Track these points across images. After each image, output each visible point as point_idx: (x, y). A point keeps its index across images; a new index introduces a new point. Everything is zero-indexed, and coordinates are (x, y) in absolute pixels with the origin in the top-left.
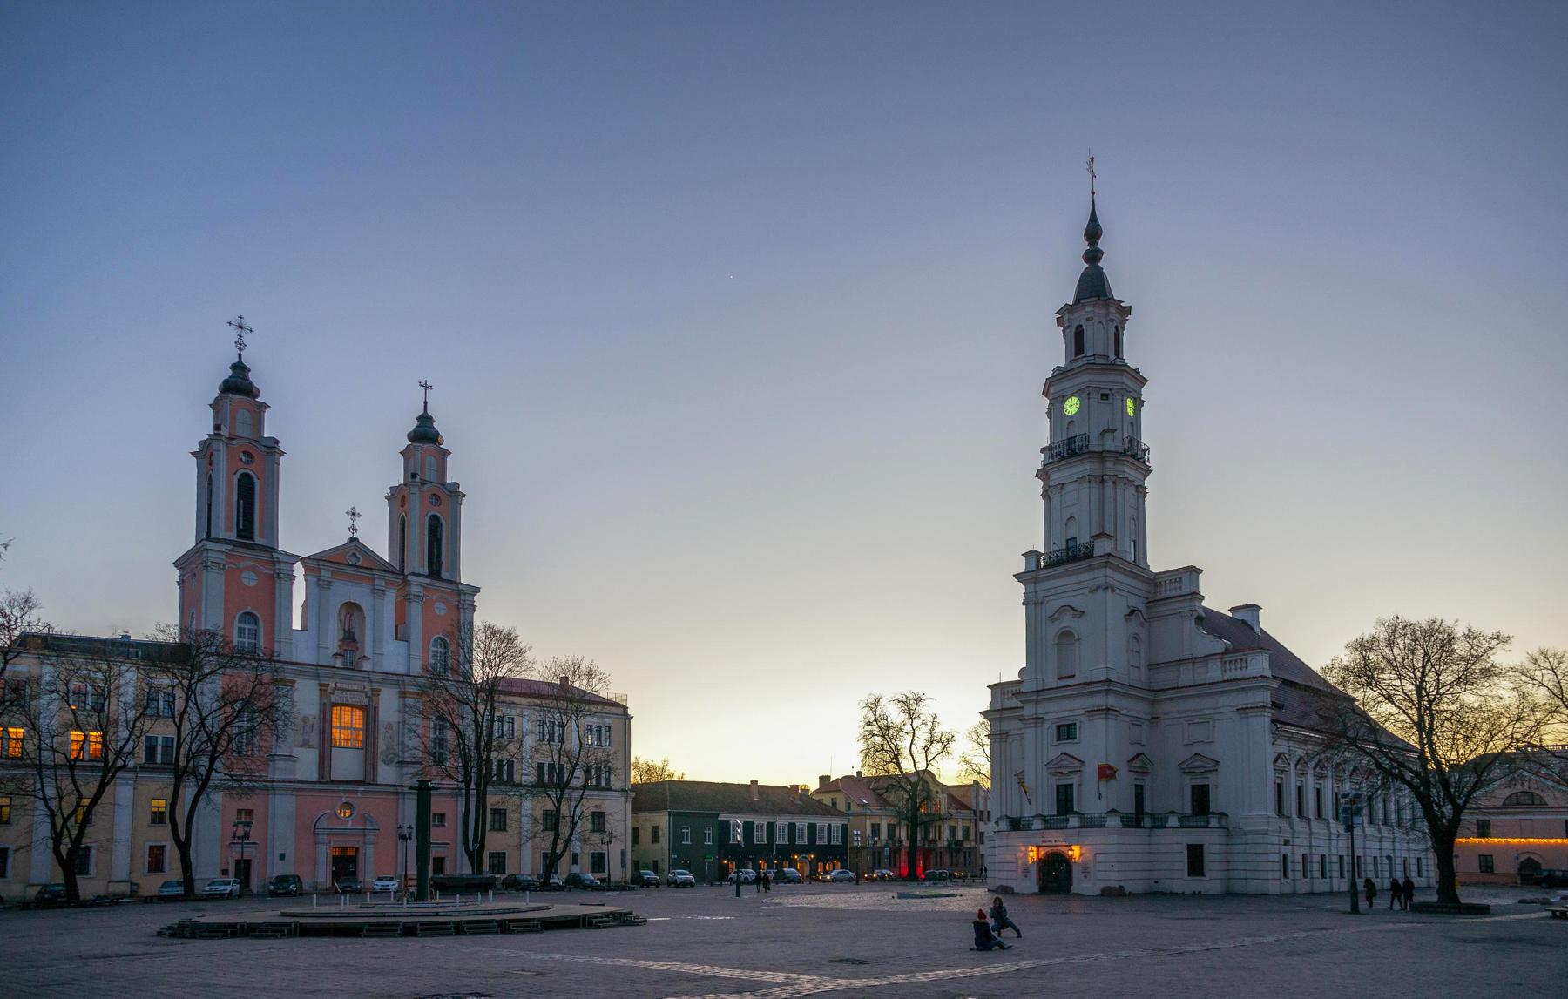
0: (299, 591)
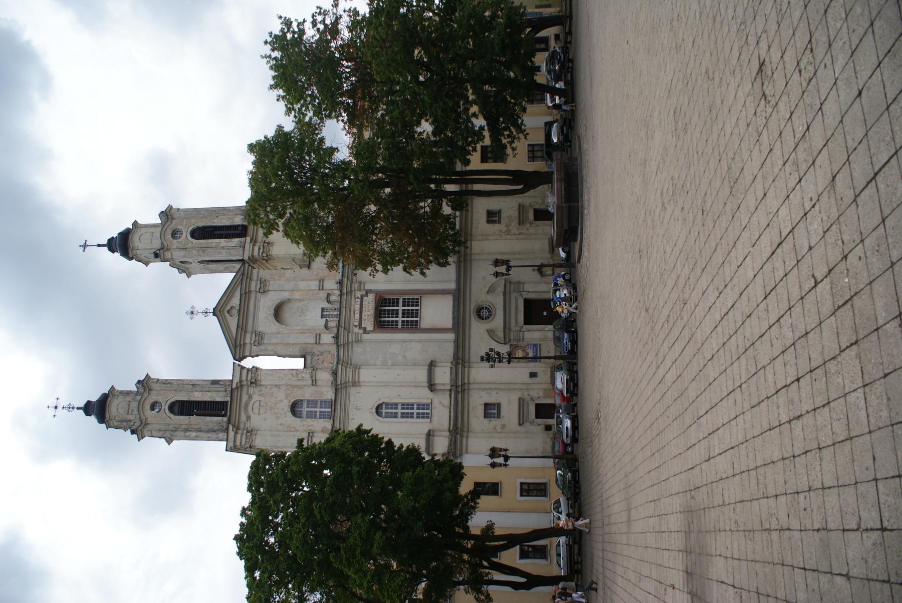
0: (266, 362)
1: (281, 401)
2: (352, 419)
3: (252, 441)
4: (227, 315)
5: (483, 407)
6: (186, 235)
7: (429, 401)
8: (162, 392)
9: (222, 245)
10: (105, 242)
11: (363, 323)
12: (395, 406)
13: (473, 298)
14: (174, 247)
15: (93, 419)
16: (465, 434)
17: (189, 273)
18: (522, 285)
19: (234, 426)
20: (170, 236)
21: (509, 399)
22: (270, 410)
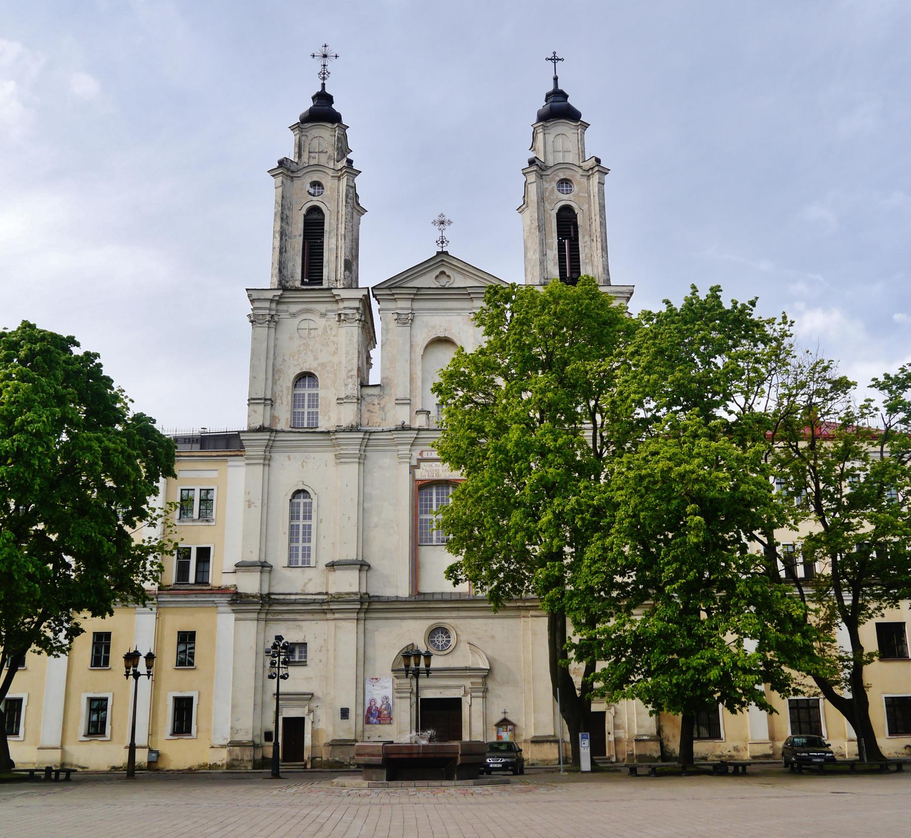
1: (316, 358)
2: (289, 458)
3: (260, 324)
4: (437, 272)
5: (301, 641)
6: (565, 199)
7: (312, 564)
8: (335, 194)
9: (549, 252)
10: (560, 88)
11: (426, 464)
12: (308, 517)
13: (462, 621)
14: (546, 185)
15: (308, 104)
16: (263, 616)
17: (523, 210)
18: (481, 694)
19: (281, 297)
20: (563, 177)
21: (312, 678)
22: (304, 344)
